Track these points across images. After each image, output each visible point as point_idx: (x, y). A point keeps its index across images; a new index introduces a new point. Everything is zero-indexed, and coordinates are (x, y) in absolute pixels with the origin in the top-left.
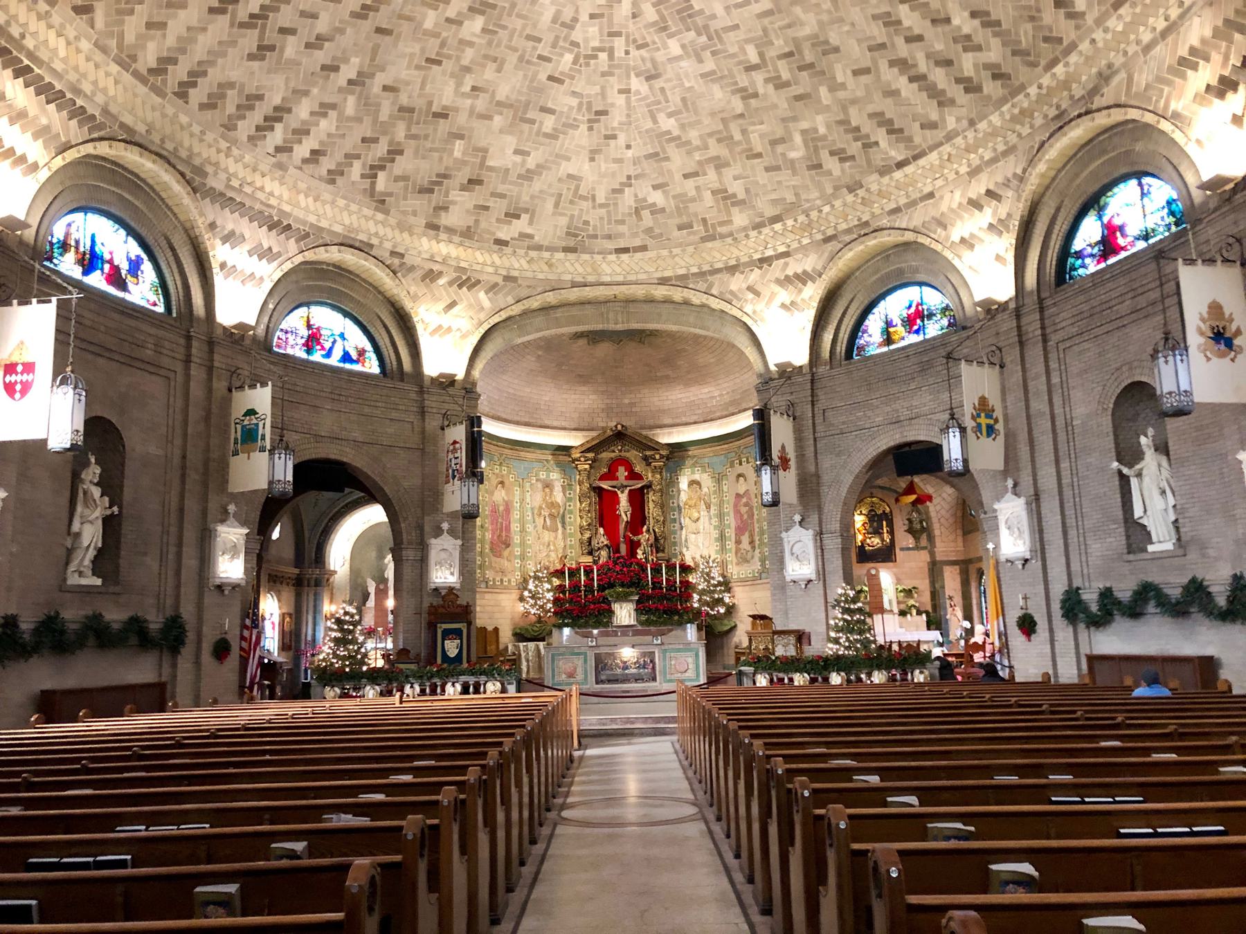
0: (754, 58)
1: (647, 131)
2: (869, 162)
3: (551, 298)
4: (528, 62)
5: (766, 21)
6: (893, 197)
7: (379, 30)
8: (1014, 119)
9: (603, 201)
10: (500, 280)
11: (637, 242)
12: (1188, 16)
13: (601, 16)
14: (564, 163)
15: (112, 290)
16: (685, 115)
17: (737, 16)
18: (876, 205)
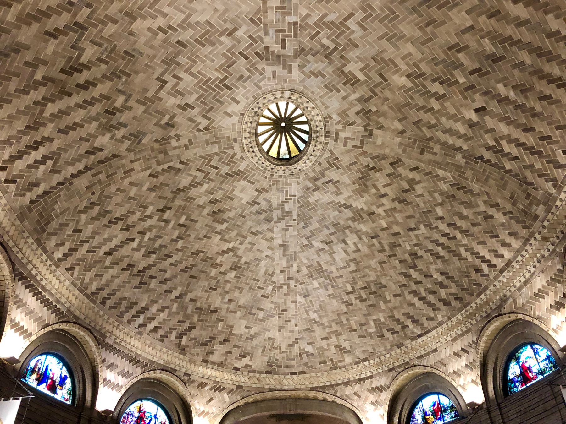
0: (350, 289)
1: (304, 319)
2: (405, 335)
3: (258, 397)
4: (253, 289)
5: (354, 274)
7: (191, 277)
9: (285, 350)
10: (234, 387)
11: (300, 370)
12: (534, 276)
13: (285, 271)
14: (267, 333)
15: (49, 393)
16: (321, 312)
17: (341, 272)
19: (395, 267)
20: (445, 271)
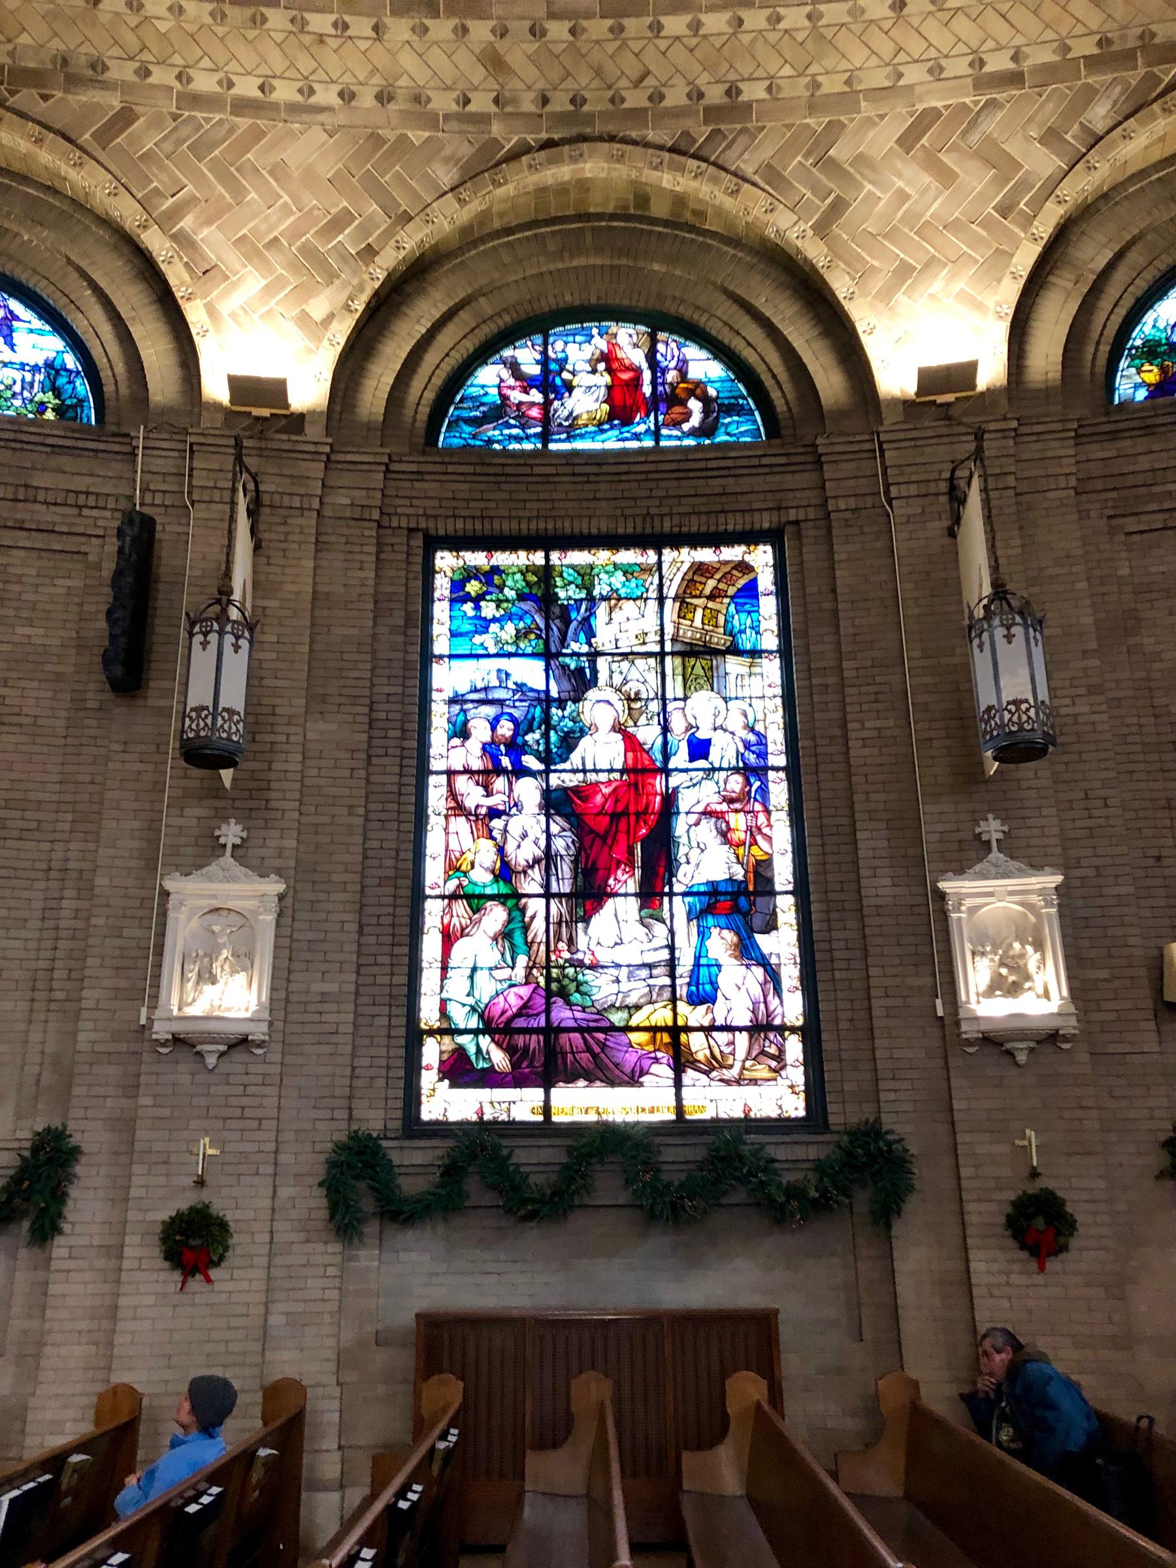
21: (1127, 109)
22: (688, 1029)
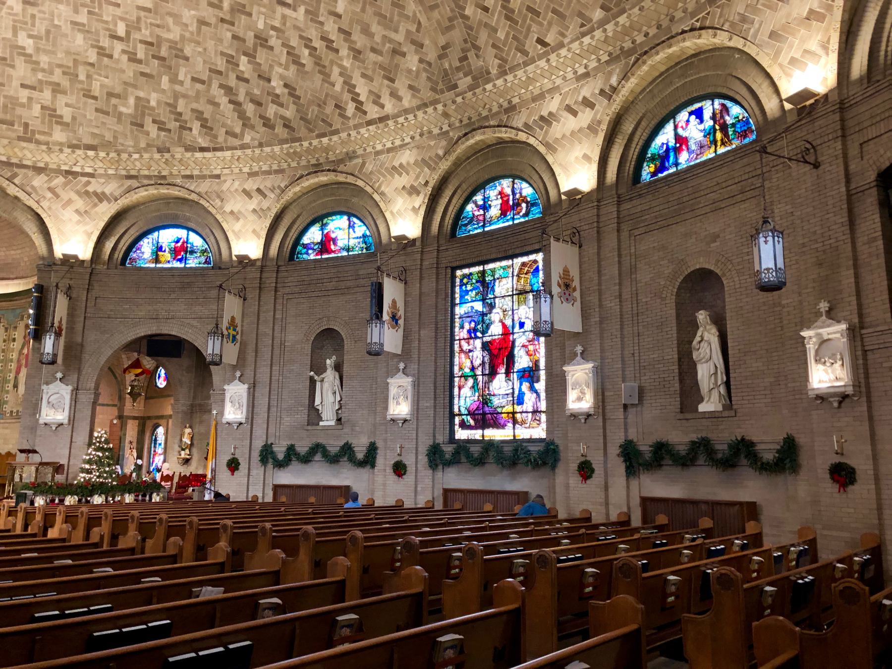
0: (121, 30)
5: (142, 14)
6: (190, 168)
8: (288, 154)
12: (404, 148)
16: (44, 42)
18: (175, 168)
19: (221, 40)
20: (294, 85)
21: (621, 77)
22: (516, 413)
